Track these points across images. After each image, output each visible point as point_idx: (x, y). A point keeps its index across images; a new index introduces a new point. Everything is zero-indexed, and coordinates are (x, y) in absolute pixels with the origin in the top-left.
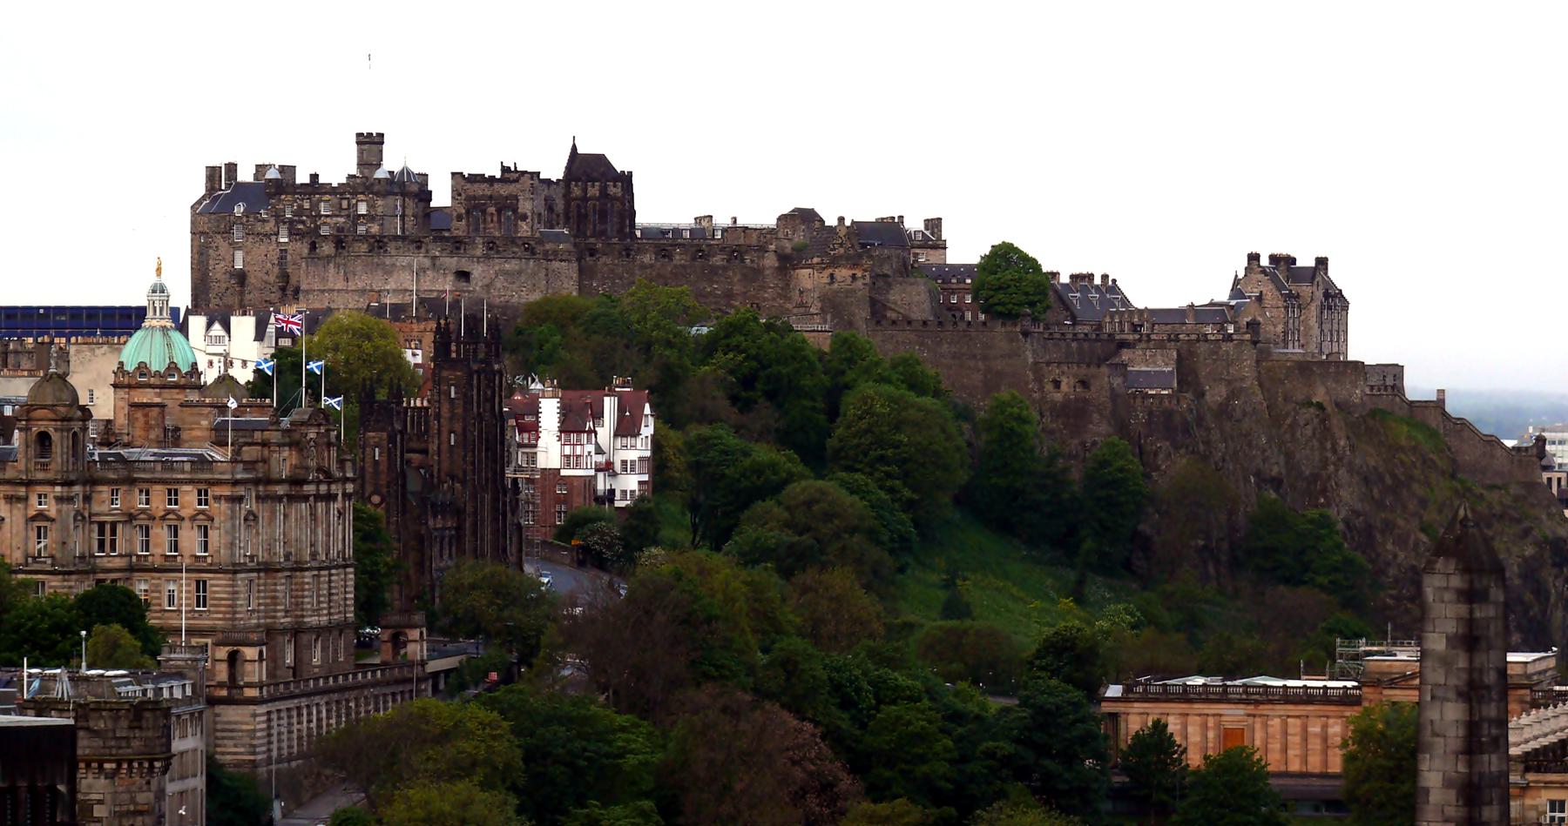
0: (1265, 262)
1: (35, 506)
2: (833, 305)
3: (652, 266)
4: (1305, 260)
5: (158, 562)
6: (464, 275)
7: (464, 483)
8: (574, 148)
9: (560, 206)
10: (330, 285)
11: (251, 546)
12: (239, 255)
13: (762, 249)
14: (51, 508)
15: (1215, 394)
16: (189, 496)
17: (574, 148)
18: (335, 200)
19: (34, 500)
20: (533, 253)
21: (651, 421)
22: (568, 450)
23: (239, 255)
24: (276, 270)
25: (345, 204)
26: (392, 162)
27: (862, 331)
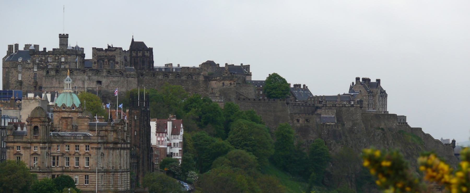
0: (361, 80)
1: (33, 150)
2: (224, 93)
3: (162, 80)
4: (373, 80)
5: (72, 169)
6: (99, 82)
7: (139, 148)
8: (133, 40)
9: (128, 59)
10: (54, 85)
11: (103, 164)
12: (20, 75)
13: (199, 74)
14: (38, 151)
15: (348, 125)
16: (83, 148)
17: (133, 40)
18: (53, 56)
19: (33, 148)
20: (123, 75)
21: (182, 130)
22: (159, 139)
23: (20, 75)
24: (33, 80)
25: (57, 58)
26: (72, 43)
27: (234, 102)
